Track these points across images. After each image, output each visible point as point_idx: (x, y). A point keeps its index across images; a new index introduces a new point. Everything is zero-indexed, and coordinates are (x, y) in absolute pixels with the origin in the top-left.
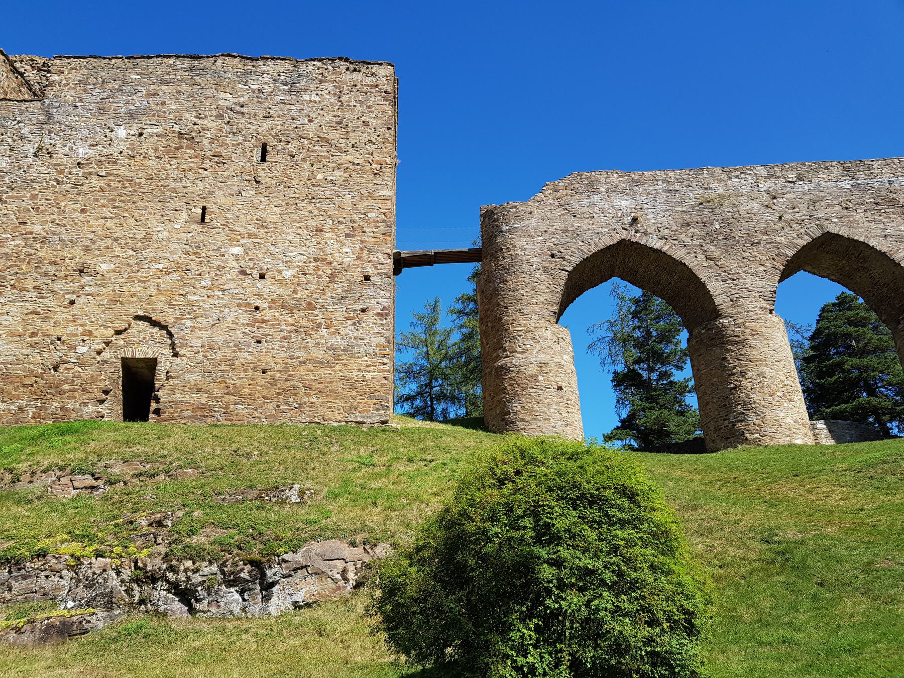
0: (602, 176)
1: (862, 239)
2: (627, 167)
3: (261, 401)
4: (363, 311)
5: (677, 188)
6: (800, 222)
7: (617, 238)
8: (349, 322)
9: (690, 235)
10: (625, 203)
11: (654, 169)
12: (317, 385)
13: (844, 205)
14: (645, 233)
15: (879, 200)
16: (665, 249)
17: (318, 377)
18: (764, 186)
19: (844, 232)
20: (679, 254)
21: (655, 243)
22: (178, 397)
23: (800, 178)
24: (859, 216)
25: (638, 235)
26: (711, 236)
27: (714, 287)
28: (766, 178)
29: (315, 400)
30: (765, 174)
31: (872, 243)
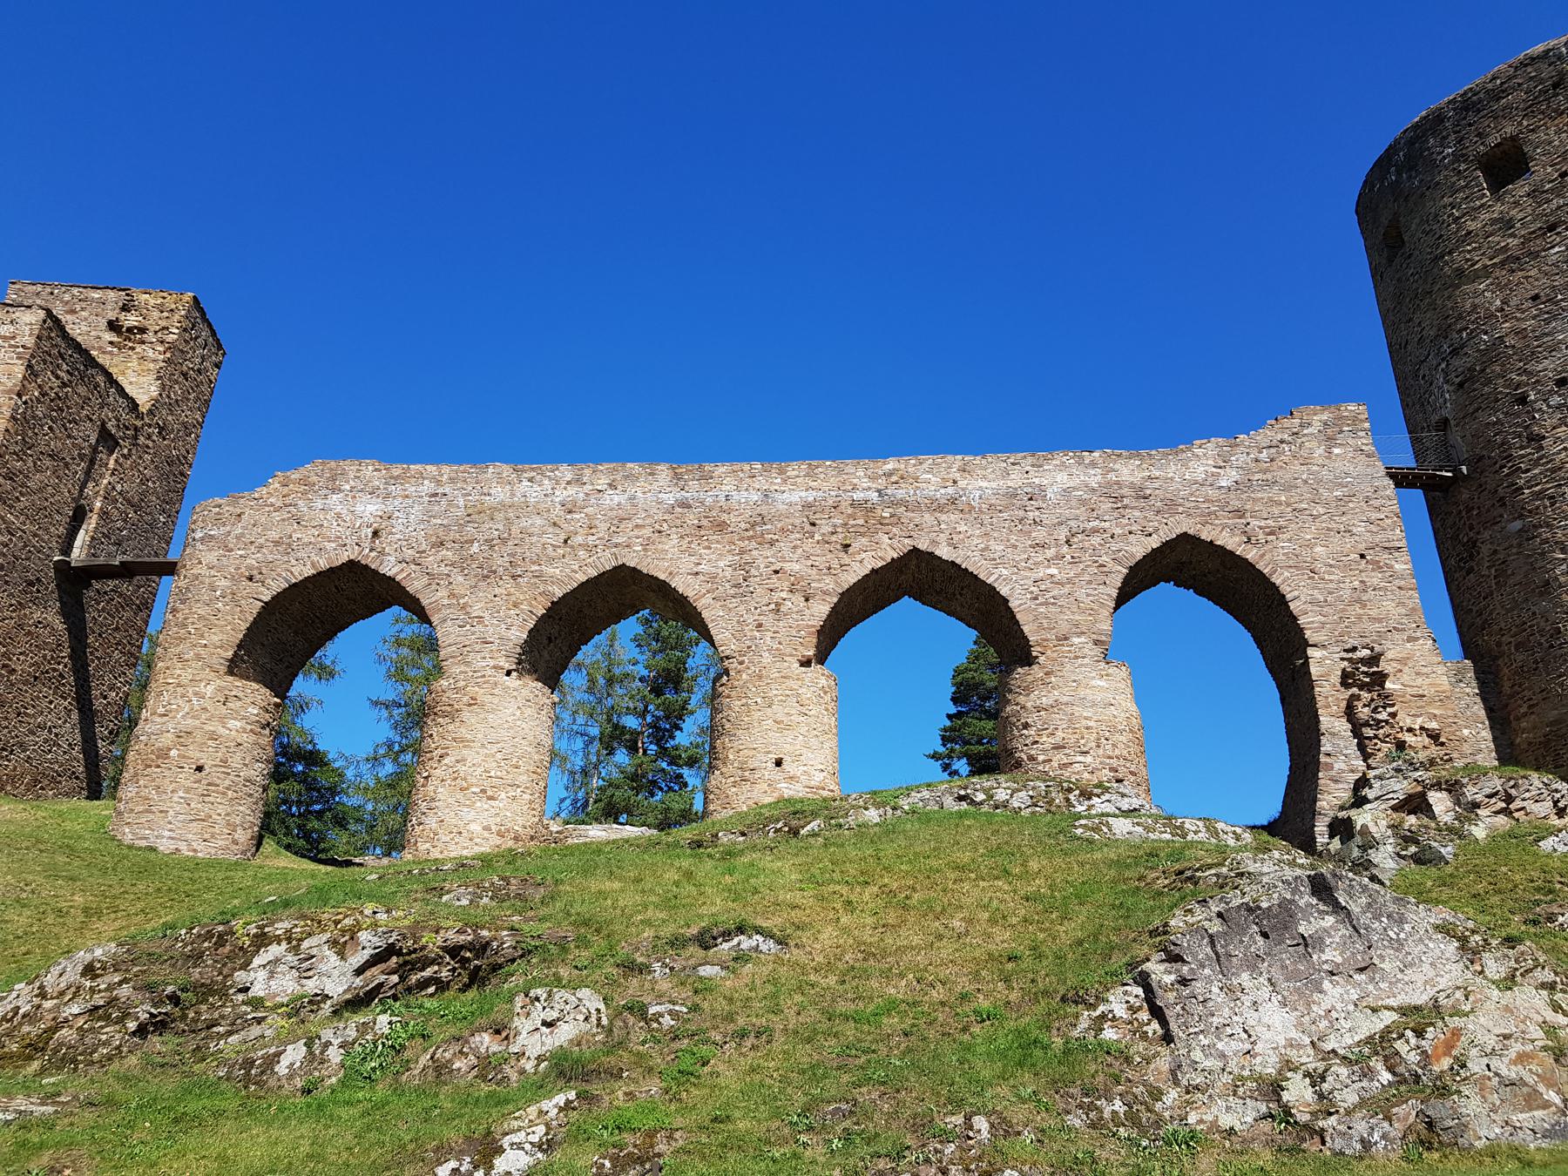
0: (350, 467)
1: (662, 577)
2: (387, 456)
5: (447, 491)
6: (590, 549)
7: (344, 557)
9: (439, 558)
10: (371, 508)
13: (657, 527)
14: (382, 553)
15: (705, 522)
16: (398, 578)
18: (561, 494)
23: (612, 486)
24: (671, 544)
25: (373, 554)
26: (461, 565)
28: (568, 483)
30: (569, 477)
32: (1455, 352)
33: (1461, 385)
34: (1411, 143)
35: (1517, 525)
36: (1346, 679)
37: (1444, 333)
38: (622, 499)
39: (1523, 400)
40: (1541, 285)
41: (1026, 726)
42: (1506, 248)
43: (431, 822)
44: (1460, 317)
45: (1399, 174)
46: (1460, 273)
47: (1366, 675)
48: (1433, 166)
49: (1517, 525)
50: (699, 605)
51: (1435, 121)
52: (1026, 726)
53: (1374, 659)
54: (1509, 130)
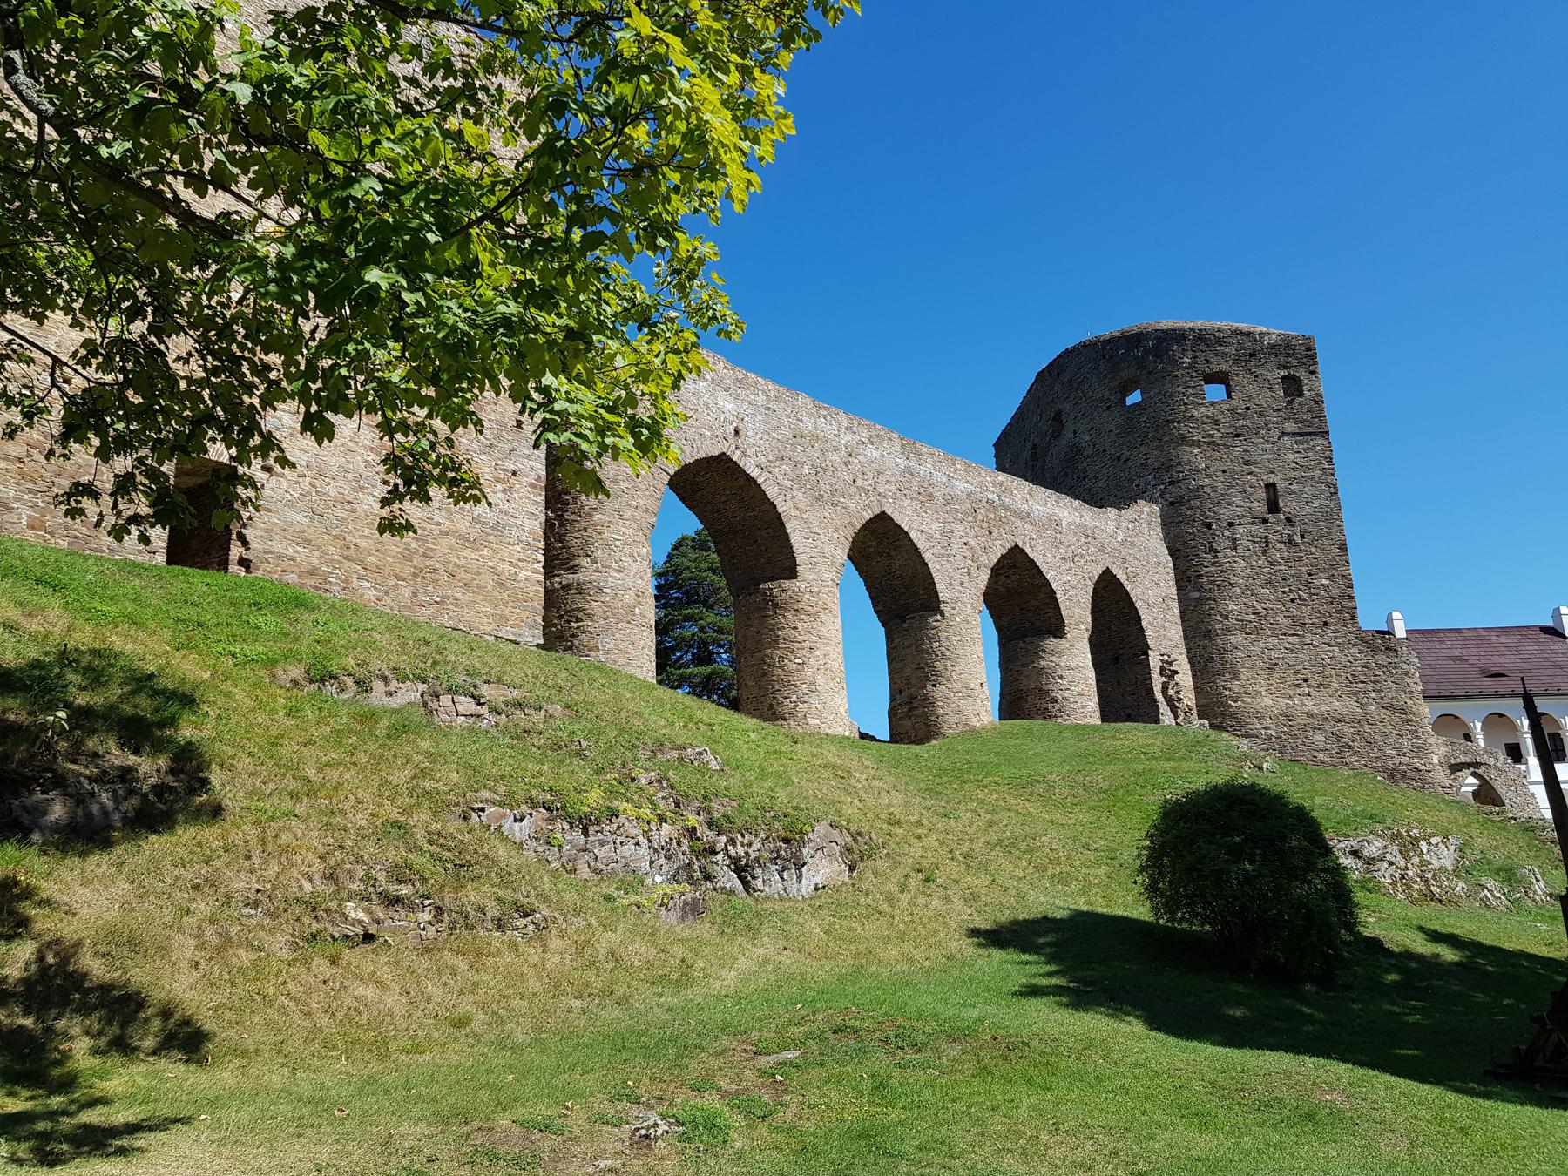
3: (392, 581)
4: (514, 473)
8: (499, 487)
11: (758, 374)
12: (463, 575)
16: (760, 481)
17: (463, 562)
19: (898, 518)
20: (772, 492)
21: (754, 473)
22: (277, 546)
27: (797, 541)
29: (459, 595)
31: (913, 535)
32: (1172, 483)
33: (1172, 503)
34: (1160, 340)
35: (1197, 595)
36: (1162, 669)
37: (1168, 469)
38: (875, 454)
39: (1209, 526)
40: (1228, 466)
41: (1061, 677)
42: (1211, 436)
43: (814, 701)
44: (1179, 464)
45: (1145, 353)
46: (1184, 438)
47: (1169, 673)
48: (1174, 363)
49: (1197, 595)
50: (927, 556)
51: (1177, 336)
52: (1061, 677)
53: (1170, 663)
54: (1224, 367)
